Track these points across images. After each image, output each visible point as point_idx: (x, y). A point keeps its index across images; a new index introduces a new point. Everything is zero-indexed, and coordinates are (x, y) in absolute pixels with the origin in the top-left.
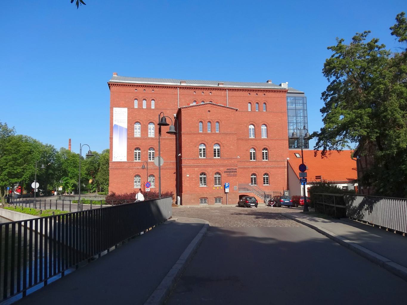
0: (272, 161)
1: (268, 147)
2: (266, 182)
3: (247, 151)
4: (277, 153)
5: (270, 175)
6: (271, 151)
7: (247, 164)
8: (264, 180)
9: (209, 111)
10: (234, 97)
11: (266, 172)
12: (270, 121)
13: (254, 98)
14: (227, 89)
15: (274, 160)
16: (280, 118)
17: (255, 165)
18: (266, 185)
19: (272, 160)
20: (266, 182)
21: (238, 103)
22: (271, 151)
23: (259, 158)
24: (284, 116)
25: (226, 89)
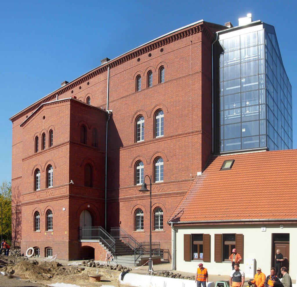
9: (44, 118)
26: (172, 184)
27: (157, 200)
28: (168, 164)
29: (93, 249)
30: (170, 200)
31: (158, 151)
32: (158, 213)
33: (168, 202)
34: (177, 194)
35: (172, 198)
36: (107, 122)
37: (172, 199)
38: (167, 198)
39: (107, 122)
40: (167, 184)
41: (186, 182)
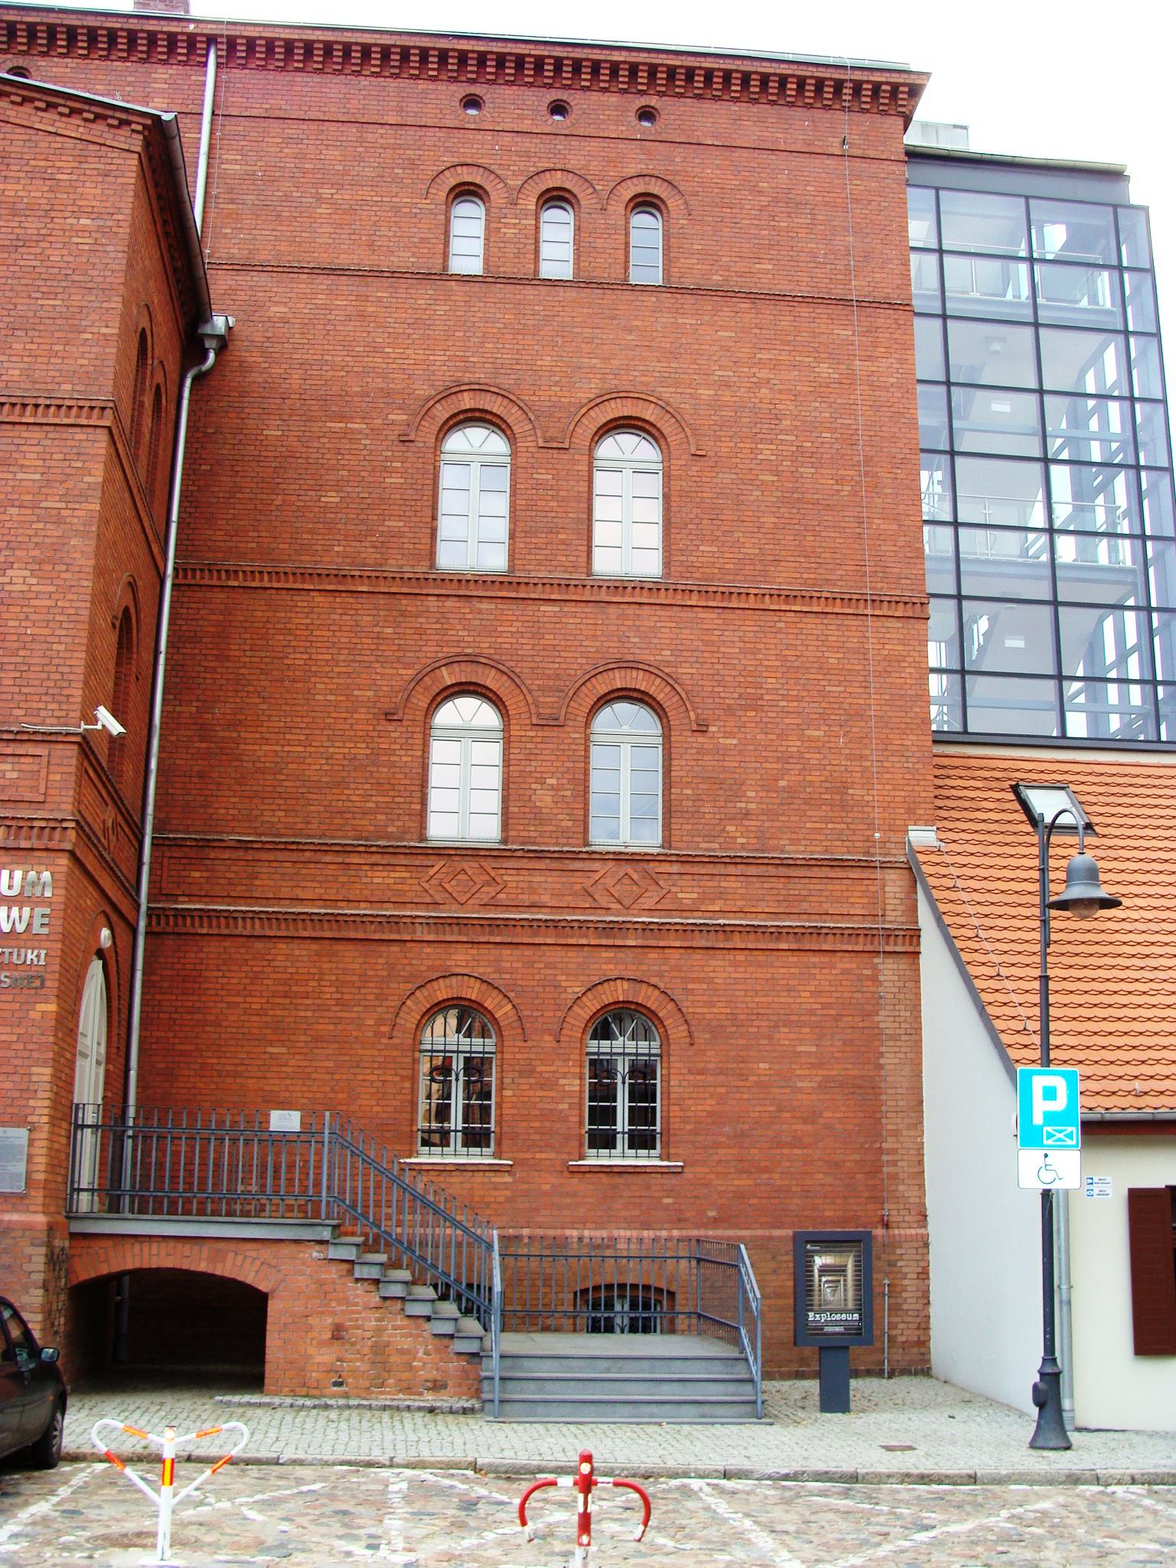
0: (714, 861)
1: (669, 681)
2: (622, 1123)
3: (388, 716)
4: (784, 759)
5: (677, 1031)
6: (702, 729)
7: (379, 877)
8: (602, 1093)
10: (293, 130)
11: (621, 992)
12: (705, 393)
13: (526, 143)
14: (211, 40)
15: (741, 841)
16: (823, 368)
17: (486, 894)
18: (621, 1156)
19: (705, 847)
20: (622, 1123)
21: (326, 192)
22: (702, 729)
23: (538, 816)
24: (875, 345)
25: (192, 40)
26: (732, 870)
27: (609, 961)
28: (701, 751)
29: (259, 1300)
30: (721, 969)
31: (630, 657)
32: (623, 1046)
33: (710, 981)
34: (779, 933)
35: (741, 957)
36: (188, 382)
37: (735, 964)
38: (697, 956)
39: (188, 382)
40: (696, 869)
41: (841, 873)
